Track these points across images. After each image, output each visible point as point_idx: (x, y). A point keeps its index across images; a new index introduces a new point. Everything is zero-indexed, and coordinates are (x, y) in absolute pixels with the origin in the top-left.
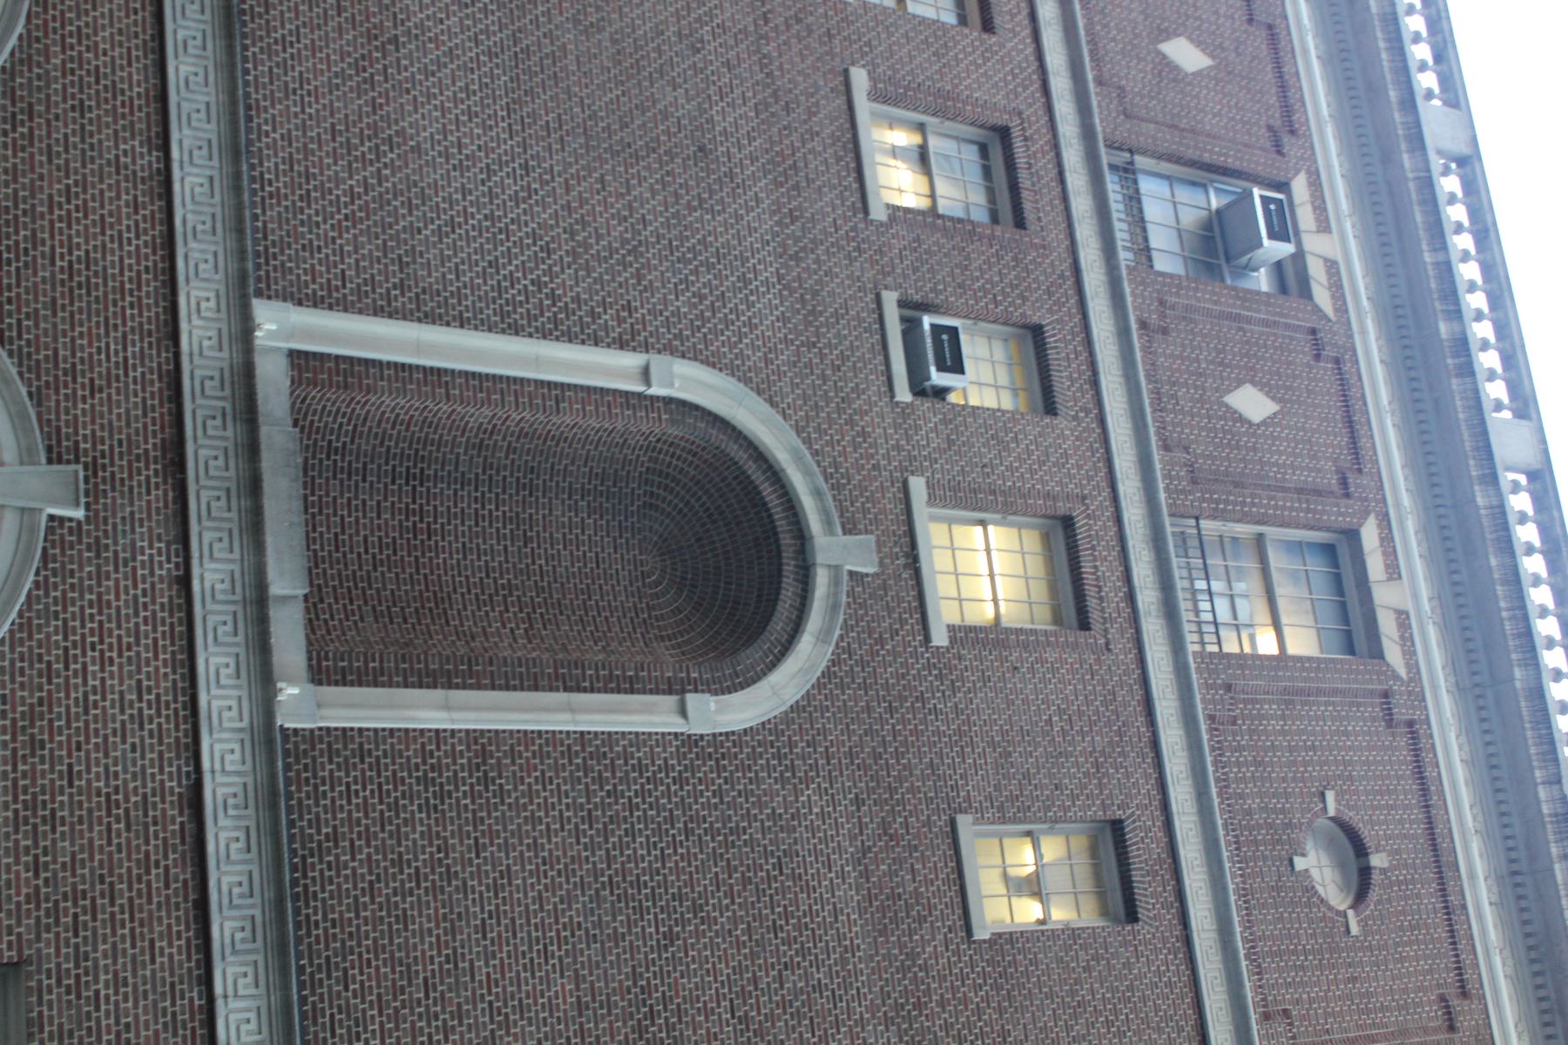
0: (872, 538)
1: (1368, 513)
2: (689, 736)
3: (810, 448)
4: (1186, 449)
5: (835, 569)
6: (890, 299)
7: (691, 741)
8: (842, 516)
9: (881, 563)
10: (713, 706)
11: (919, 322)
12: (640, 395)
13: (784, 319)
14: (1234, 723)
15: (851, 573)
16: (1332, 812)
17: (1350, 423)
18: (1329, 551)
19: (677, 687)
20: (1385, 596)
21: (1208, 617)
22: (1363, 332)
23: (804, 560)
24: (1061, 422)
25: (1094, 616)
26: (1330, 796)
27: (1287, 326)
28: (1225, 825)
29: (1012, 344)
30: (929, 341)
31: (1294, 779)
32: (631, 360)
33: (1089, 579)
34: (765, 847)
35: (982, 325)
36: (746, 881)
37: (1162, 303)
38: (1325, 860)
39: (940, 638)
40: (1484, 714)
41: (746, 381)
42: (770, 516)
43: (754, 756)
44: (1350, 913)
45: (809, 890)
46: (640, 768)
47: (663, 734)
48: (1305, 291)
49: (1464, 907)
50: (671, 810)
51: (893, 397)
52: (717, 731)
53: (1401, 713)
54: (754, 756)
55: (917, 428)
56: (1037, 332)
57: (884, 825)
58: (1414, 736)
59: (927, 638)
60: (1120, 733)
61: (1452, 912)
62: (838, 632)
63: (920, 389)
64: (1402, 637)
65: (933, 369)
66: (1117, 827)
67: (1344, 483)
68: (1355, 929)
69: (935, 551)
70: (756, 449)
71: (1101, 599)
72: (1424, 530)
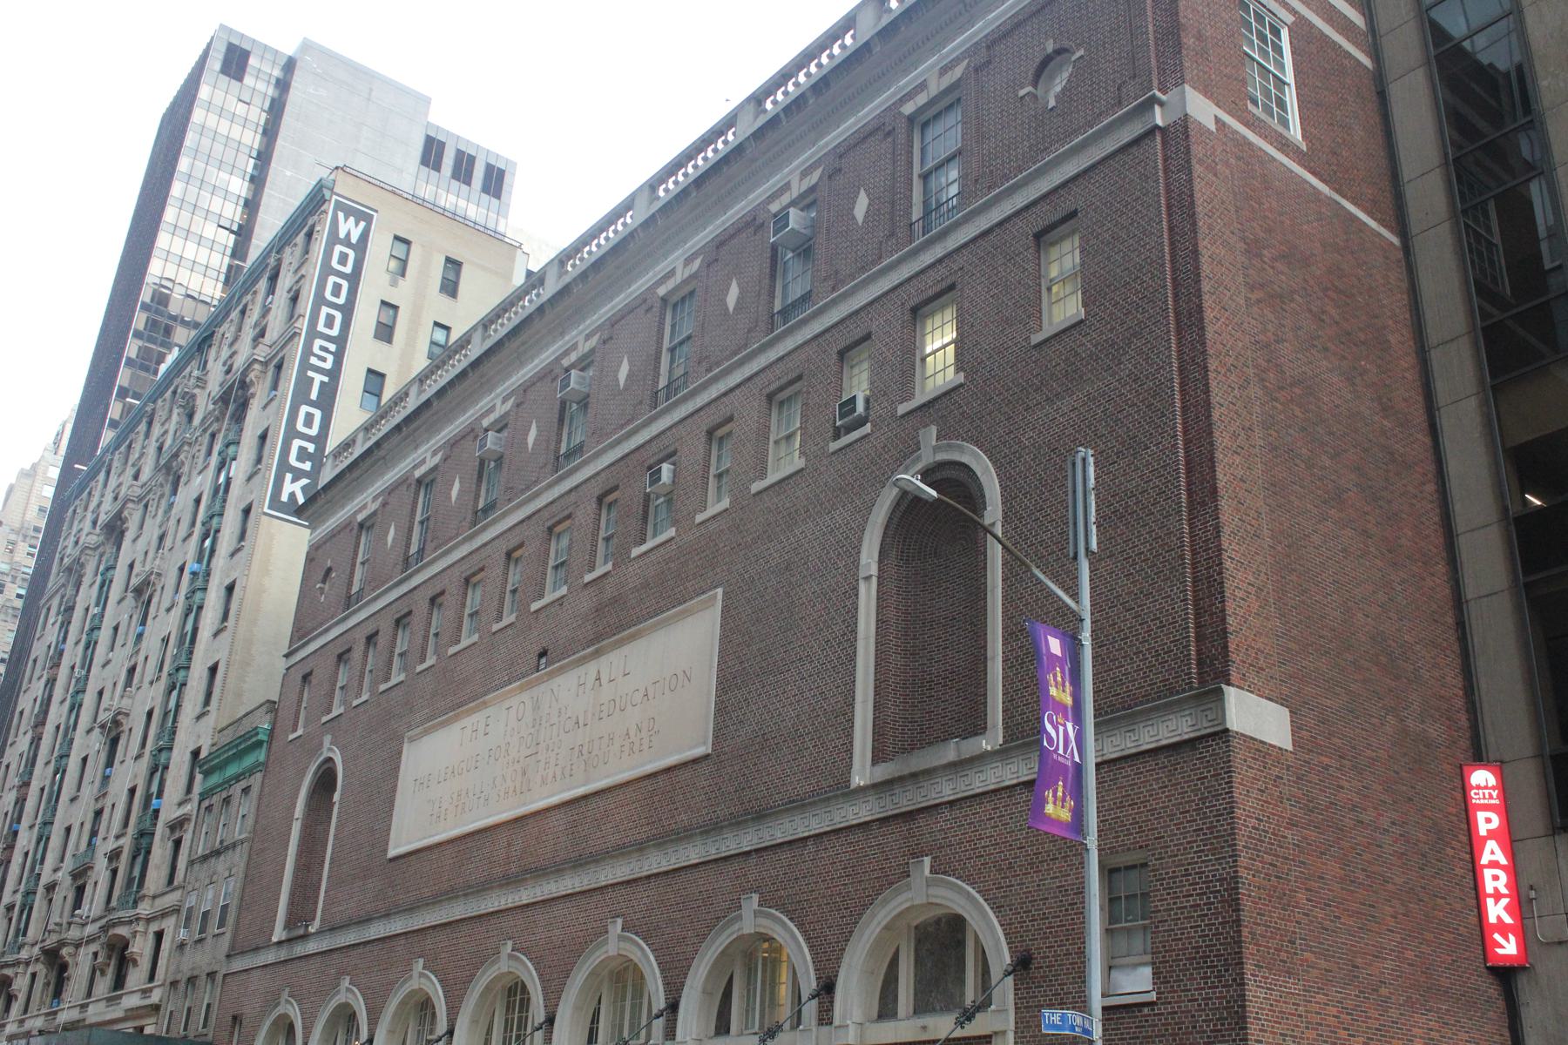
5: (936, 449)
16: (1030, 89)
17: (865, 138)
18: (925, 125)
25: (949, 282)
26: (1022, 93)
39: (961, 378)
48: (812, 189)
59: (961, 385)
63: (861, 422)
66: (1038, 236)
67: (889, 134)
68: (1081, 52)
72: (906, 72)
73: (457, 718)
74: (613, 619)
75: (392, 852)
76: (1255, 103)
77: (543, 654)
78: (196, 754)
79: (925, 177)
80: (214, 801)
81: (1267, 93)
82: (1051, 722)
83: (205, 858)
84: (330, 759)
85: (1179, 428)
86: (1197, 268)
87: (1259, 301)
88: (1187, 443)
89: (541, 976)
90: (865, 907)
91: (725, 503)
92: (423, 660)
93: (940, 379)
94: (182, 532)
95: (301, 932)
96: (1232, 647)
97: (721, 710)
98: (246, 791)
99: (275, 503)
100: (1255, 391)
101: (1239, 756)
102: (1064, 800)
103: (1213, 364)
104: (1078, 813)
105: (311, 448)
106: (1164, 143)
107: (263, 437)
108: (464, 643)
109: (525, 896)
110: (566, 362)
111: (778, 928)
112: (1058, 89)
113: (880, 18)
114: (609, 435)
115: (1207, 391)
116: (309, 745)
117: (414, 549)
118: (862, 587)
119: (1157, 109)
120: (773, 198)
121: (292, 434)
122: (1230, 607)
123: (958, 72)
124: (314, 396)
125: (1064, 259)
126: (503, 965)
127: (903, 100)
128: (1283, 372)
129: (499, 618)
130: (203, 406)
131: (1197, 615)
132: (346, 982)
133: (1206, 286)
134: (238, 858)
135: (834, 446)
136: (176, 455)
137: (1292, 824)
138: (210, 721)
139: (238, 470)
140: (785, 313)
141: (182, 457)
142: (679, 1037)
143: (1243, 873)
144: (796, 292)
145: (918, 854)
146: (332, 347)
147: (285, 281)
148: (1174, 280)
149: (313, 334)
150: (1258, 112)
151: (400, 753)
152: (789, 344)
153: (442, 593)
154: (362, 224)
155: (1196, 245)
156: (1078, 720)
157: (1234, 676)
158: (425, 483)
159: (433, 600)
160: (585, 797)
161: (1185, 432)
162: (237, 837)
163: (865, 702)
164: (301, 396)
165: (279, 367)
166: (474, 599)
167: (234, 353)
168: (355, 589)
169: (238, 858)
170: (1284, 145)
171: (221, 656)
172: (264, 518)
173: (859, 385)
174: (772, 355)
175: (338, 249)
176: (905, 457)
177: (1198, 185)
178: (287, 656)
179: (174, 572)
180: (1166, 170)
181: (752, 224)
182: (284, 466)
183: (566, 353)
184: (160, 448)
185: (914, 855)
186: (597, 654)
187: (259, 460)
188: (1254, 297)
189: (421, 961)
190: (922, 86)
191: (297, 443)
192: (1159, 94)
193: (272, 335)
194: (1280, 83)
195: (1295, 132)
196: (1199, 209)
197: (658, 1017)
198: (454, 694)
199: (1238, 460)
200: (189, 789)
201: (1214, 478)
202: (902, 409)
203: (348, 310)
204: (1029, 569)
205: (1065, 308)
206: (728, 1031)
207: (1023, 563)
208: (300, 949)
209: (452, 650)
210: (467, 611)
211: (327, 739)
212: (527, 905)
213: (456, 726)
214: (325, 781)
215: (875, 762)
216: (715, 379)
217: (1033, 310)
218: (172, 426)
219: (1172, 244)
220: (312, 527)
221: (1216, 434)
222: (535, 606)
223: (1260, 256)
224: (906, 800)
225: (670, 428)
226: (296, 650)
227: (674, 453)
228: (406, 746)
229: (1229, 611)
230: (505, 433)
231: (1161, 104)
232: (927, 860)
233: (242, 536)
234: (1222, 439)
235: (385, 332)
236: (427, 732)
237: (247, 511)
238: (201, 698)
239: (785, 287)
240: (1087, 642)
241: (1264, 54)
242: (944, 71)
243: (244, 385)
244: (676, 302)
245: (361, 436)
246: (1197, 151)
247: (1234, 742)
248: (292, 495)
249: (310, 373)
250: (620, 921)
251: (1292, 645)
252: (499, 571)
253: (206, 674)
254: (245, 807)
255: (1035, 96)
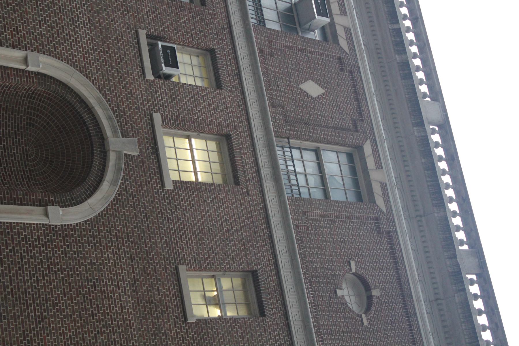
0: (136, 139)
1: (367, 139)
2: (50, 225)
3: (106, 98)
4: (283, 107)
5: (119, 153)
6: (143, 34)
7: (51, 228)
8: (121, 129)
9: (141, 151)
10: (61, 212)
11: (157, 45)
12: (23, 71)
13: (92, 39)
14: (308, 229)
15: (126, 155)
16: (353, 270)
17: (357, 99)
19: (43, 204)
20: (375, 176)
21: (294, 182)
22: (363, 60)
23: (104, 149)
24: (224, 92)
25: (241, 179)
26: (353, 263)
27: (328, 56)
28: (304, 274)
29: (200, 59)
30: (161, 53)
31: (336, 255)
32: (19, 54)
33: (239, 163)
34: (87, 277)
35: (186, 48)
36: (78, 293)
37: (270, 42)
38: (351, 293)
40: (421, 228)
41: (75, 66)
42: (87, 128)
43: (81, 236)
44: (363, 316)
45: (108, 297)
46: (26, 239)
47: (37, 224)
49: (415, 314)
50: (41, 259)
51: (144, 77)
52: (63, 224)
53: (384, 228)
54: (81, 236)
55: (156, 92)
56: (212, 52)
57: (144, 269)
58: (390, 238)
59: (163, 186)
60: (254, 231)
61: (410, 316)
62: (120, 181)
64: (383, 194)
65: (163, 65)
66: (254, 274)
67: (355, 125)
68: (366, 323)
69: (167, 149)
70: (80, 98)
71: (244, 171)
72: (391, 148)
190: (379, 165)
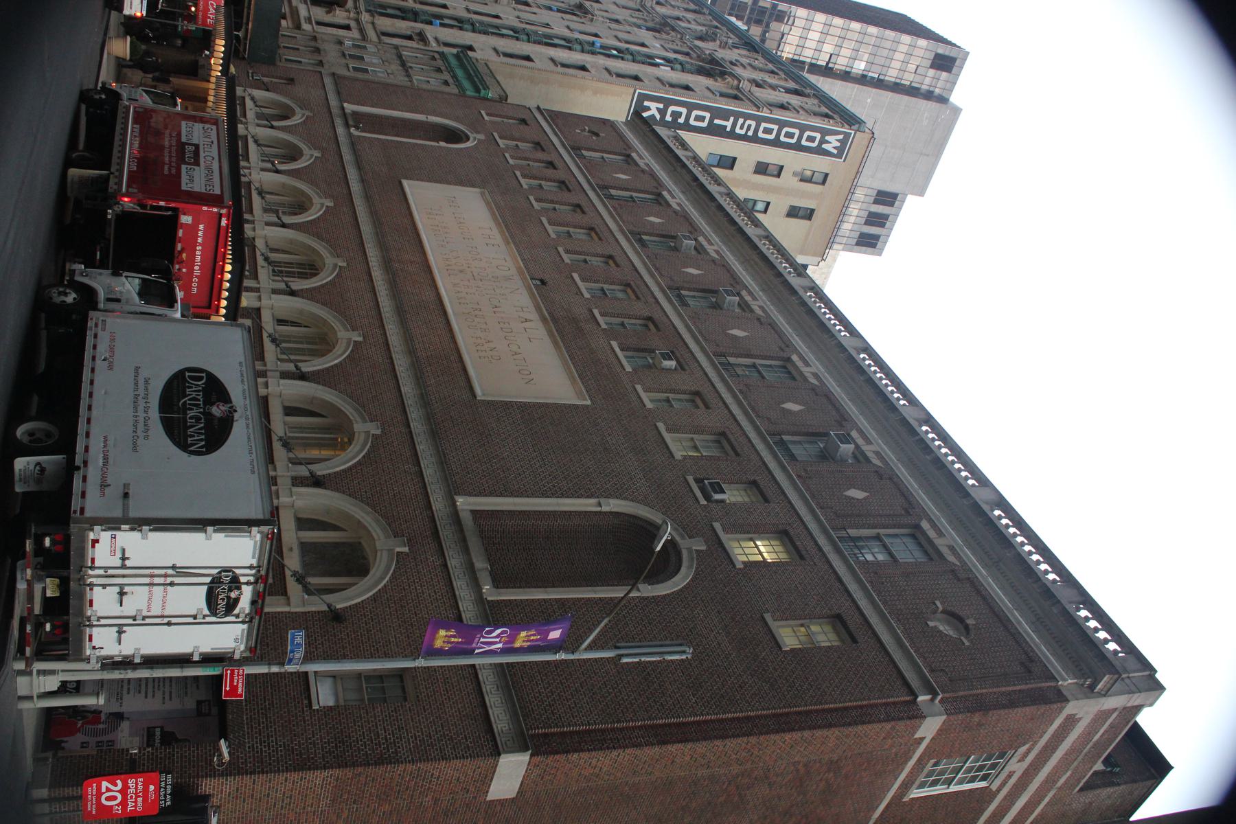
5: (689, 550)
18: (913, 536)
26: (938, 603)
48: (868, 460)
59: (734, 566)
63: (707, 497)
67: (907, 512)
68: (967, 644)
72: (950, 523)
73: (498, 224)
74: (567, 330)
75: (405, 183)
76: (935, 764)
77: (543, 282)
78: (471, 48)
79: (878, 538)
80: (439, 62)
81: (942, 773)
82: (502, 633)
83: (400, 56)
84: (468, 139)
85: (708, 717)
86: (819, 727)
87: (798, 771)
88: (698, 723)
89: (322, 286)
90: (373, 507)
91: (649, 405)
92: (537, 200)
93: (738, 551)
94: (621, 35)
95: (351, 123)
96: (557, 757)
97: (507, 405)
98: (446, 83)
99: (643, 97)
100: (735, 769)
101: (482, 763)
102: (449, 642)
103: (753, 740)
104: (440, 653)
105: (681, 120)
106: (906, 702)
107: (687, 88)
108: (550, 229)
109: (377, 274)
110: (744, 293)
111: (358, 448)
112: (941, 628)
113: (987, 503)
114: (694, 323)
115: (734, 736)
116: (477, 124)
117: (613, 192)
118: (593, 501)
119: (929, 697)
120: (861, 432)
121: (691, 107)
122: (585, 755)
123: (951, 558)
124: (716, 121)
125: (824, 635)
126: (329, 260)
127: (931, 521)
128: (748, 788)
129: (567, 252)
130: (708, 47)
131: (578, 732)
132: (317, 154)
133: (807, 733)
134: (401, 79)
135: (690, 479)
136: (673, 29)
137: (436, 800)
138: (492, 57)
139: (665, 72)
140: (782, 443)
141: (673, 34)
142: (282, 381)
143: (401, 767)
144: (797, 450)
145: (410, 542)
146: (750, 133)
147: (795, 100)
148: (811, 712)
149: (759, 120)
150: (929, 767)
151: (473, 186)
152: (760, 446)
153: (583, 212)
154: (835, 152)
155: (835, 726)
156: (506, 651)
157: (537, 759)
158: (659, 200)
159: (578, 206)
160: (445, 313)
161: (706, 722)
162: (415, 78)
163: (515, 505)
164: (716, 113)
165: (736, 97)
166: (579, 234)
167: (744, 67)
168: (584, 152)
169: (401, 79)
170: (906, 786)
171: (538, 63)
172: (632, 90)
173: (733, 495)
174: (752, 435)
175: (818, 136)
176: (684, 529)
177: (877, 726)
178: (538, 108)
179: (594, 31)
180: (887, 704)
181: (843, 419)
182: (668, 102)
183: (750, 293)
184: (678, 19)
185: (409, 540)
186: (544, 319)
187: (672, 85)
188: (800, 767)
189: (331, 204)
190: (940, 534)
191: (684, 111)
192: (939, 698)
193: (758, 92)
194: (949, 782)
195: (916, 793)
196: (860, 728)
197: (296, 366)
198: (514, 222)
199: (687, 758)
200: (447, 45)
201: (674, 742)
202: (717, 525)
203: (776, 143)
204: (608, 615)
205: (789, 637)
206: (287, 415)
207: (611, 612)
208: (339, 122)
209: (544, 220)
210: (571, 230)
211: (482, 137)
212: (371, 276)
213: (491, 224)
214: (454, 136)
215: (473, 512)
216: (735, 396)
217: (787, 615)
218: (693, 26)
219: (836, 710)
220: (627, 123)
221: (704, 743)
222: (575, 275)
223: (829, 771)
224: (447, 534)
225: (700, 366)
226: (542, 114)
227: (683, 369)
228: (477, 190)
229: (582, 755)
230: (694, 253)
231: (932, 700)
232: (406, 549)
233: (619, 75)
234: (701, 747)
235: (762, 169)
236: (488, 203)
237: (636, 78)
238: (509, 51)
239: (800, 442)
240: (557, 657)
241: (969, 770)
242: (952, 548)
243: (723, 74)
244: (786, 366)
245: (690, 154)
246: (901, 725)
247: (491, 760)
248: (648, 109)
249: (732, 119)
250: (361, 339)
251: (559, 798)
252: (599, 251)
253: (525, 53)
254: (434, 83)
255: (935, 612)
